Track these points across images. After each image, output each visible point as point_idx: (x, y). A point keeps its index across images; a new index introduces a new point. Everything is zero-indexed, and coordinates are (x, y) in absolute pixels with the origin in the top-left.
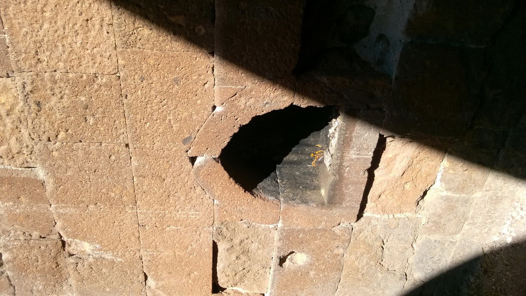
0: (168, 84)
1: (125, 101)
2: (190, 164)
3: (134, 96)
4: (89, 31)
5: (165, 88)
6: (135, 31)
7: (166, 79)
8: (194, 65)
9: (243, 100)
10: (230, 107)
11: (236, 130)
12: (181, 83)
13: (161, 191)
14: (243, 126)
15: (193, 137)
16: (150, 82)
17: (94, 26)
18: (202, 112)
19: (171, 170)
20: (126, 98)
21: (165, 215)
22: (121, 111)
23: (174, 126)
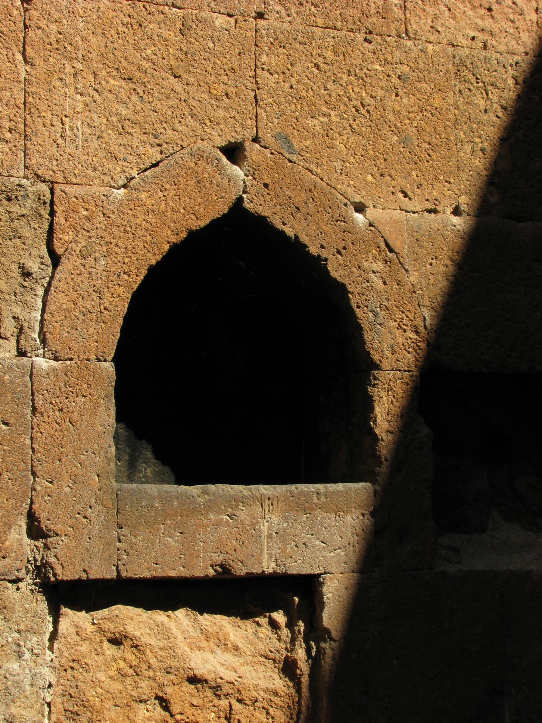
0: (399, 125)
1: (360, 37)
2: (222, 142)
3: (371, 55)
4: (474, 8)
5: (391, 117)
6: (480, 85)
7: (407, 122)
8: (436, 178)
9: (378, 266)
10: (365, 239)
11: (314, 250)
12: (402, 149)
13: (146, 65)
14: (325, 266)
15: (294, 158)
16: (400, 92)
17: (482, 17)
18: (352, 182)
19: (206, 96)
20: (366, 40)
21: (71, 59)
22: (339, 24)
23: (316, 122)
